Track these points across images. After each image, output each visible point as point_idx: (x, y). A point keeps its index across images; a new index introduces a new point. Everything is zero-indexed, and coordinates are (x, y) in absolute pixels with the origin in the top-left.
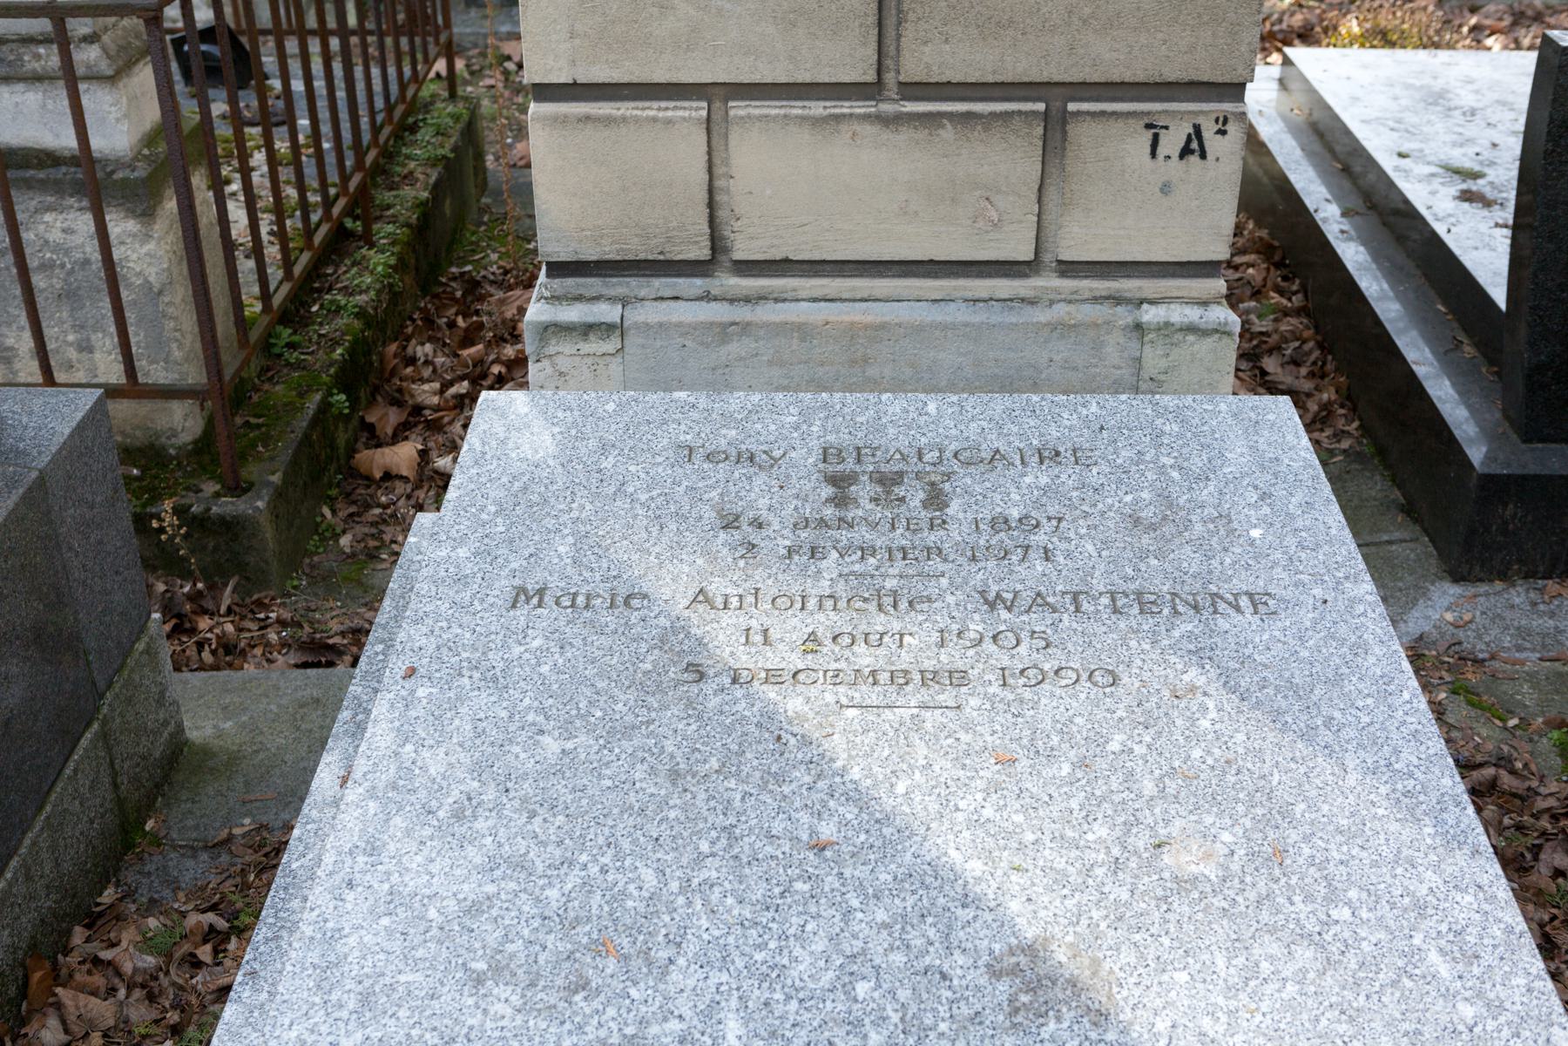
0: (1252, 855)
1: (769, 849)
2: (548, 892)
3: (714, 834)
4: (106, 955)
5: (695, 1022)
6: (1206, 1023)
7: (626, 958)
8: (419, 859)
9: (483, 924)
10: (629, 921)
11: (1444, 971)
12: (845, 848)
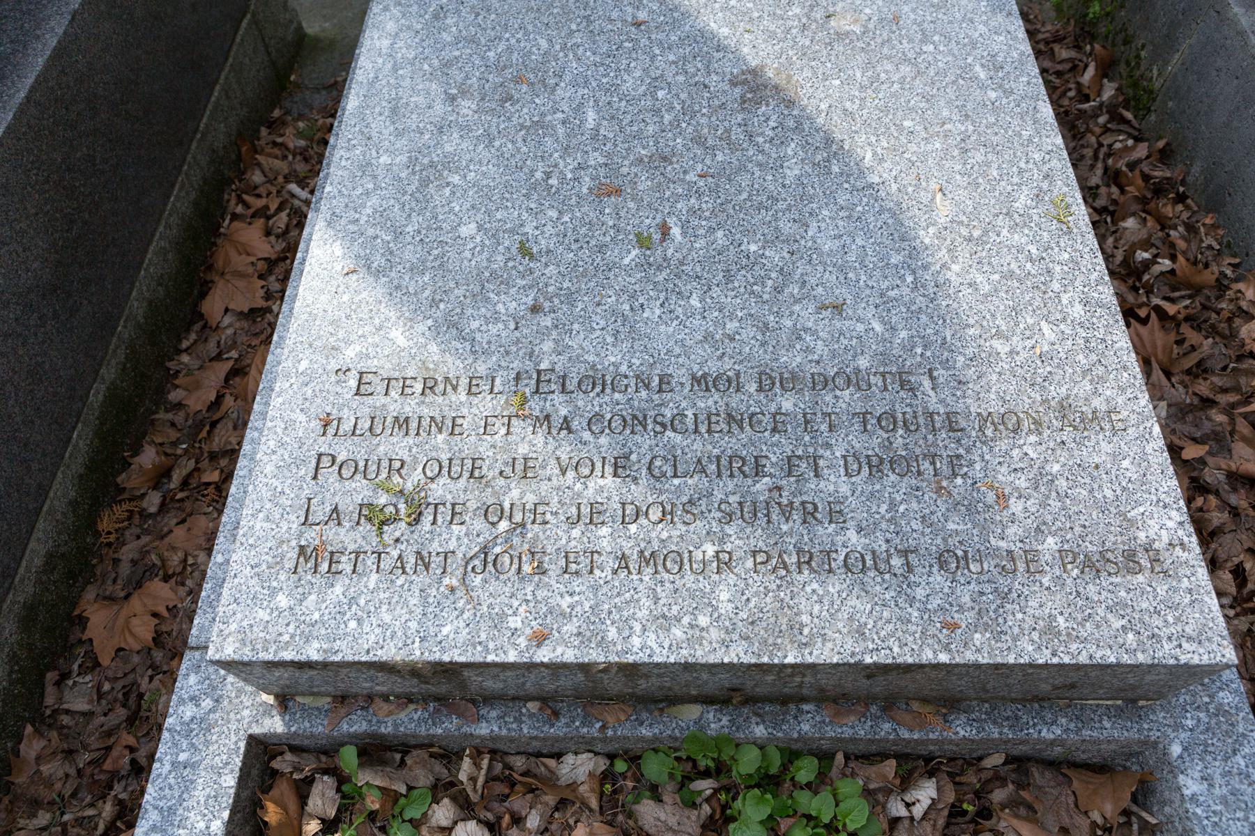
0: (881, 20)
1: (610, 27)
2: (488, 53)
3: (579, 20)
4: (279, 140)
5: (571, 113)
6: (848, 105)
7: (532, 84)
8: (417, 40)
9: (454, 71)
10: (533, 66)
11: (982, 75)
12: (652, 24)
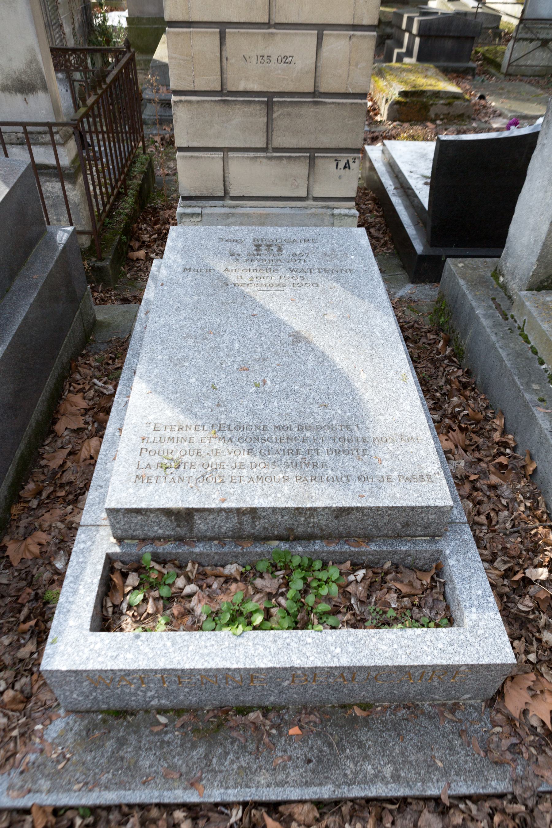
0: (343, 317)
4: (87, 362)
6: (331, 344)
11: (379, 335)
